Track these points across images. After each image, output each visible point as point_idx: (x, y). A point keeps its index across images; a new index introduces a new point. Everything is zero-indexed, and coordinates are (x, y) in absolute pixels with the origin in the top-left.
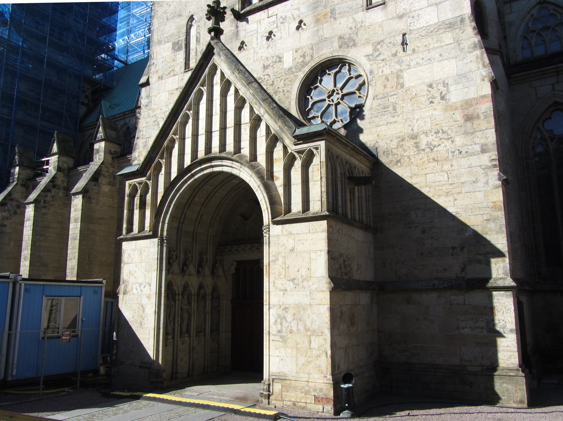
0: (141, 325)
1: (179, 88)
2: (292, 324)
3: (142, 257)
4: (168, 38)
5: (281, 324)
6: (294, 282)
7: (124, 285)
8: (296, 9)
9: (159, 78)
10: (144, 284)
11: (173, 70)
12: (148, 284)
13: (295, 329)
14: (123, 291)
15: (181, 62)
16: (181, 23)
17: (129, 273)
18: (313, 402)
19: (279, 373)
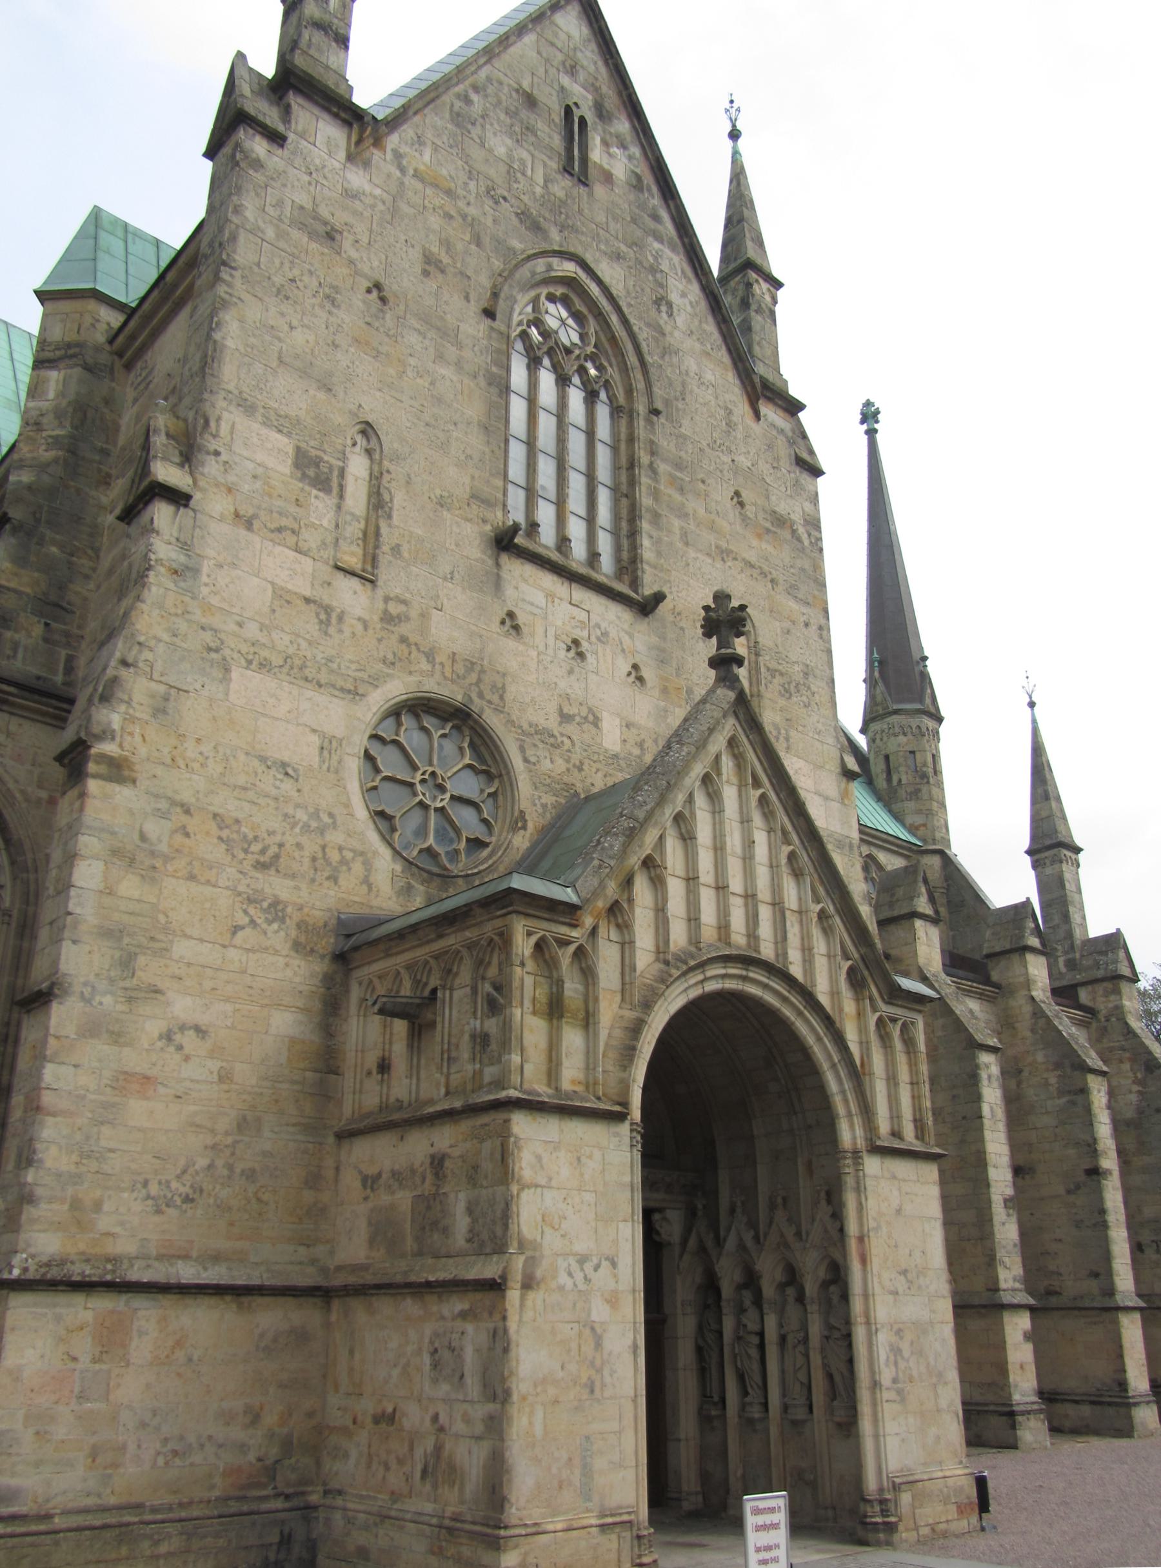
0: (592, 1391)
1: (315, 602)
2: (911, 1364)
3: (582, 1175)
4: (282, 421)
5: (896, 1363)
6: (906, 1277)
7: (522, 1259)
8: (626, 633)
9: (237, 515)
10: (595, 1260)
11: (293, 532)
12: (607, 1259)
13: (915, 1373)
14: (519, 1277)
15: (326, 529)
16: (332, 416)
17: (539, 1218)
18: (956, 1516)
19: (902, 1471)
